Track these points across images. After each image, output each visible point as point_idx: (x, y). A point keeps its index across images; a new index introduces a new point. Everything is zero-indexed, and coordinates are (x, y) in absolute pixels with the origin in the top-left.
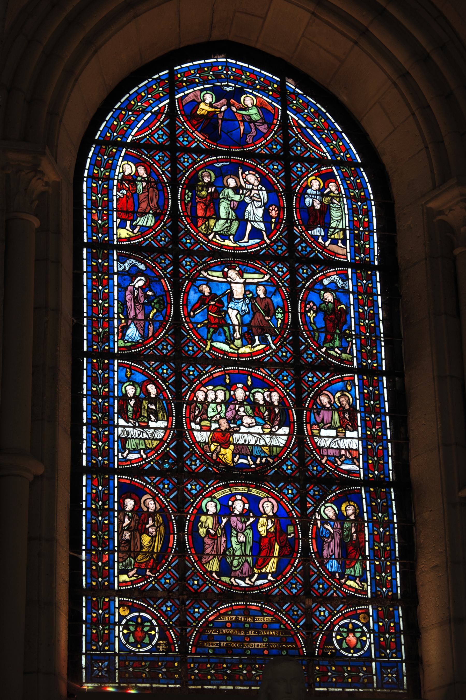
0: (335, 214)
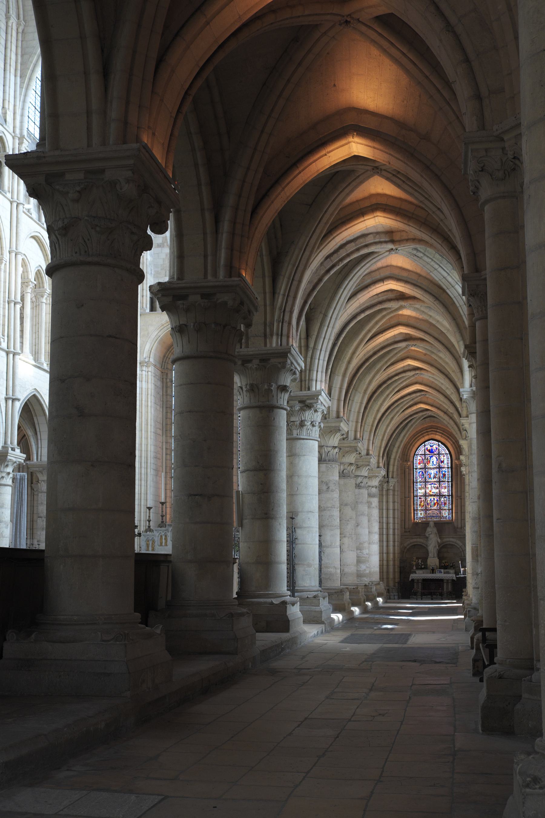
0: (445, 461)
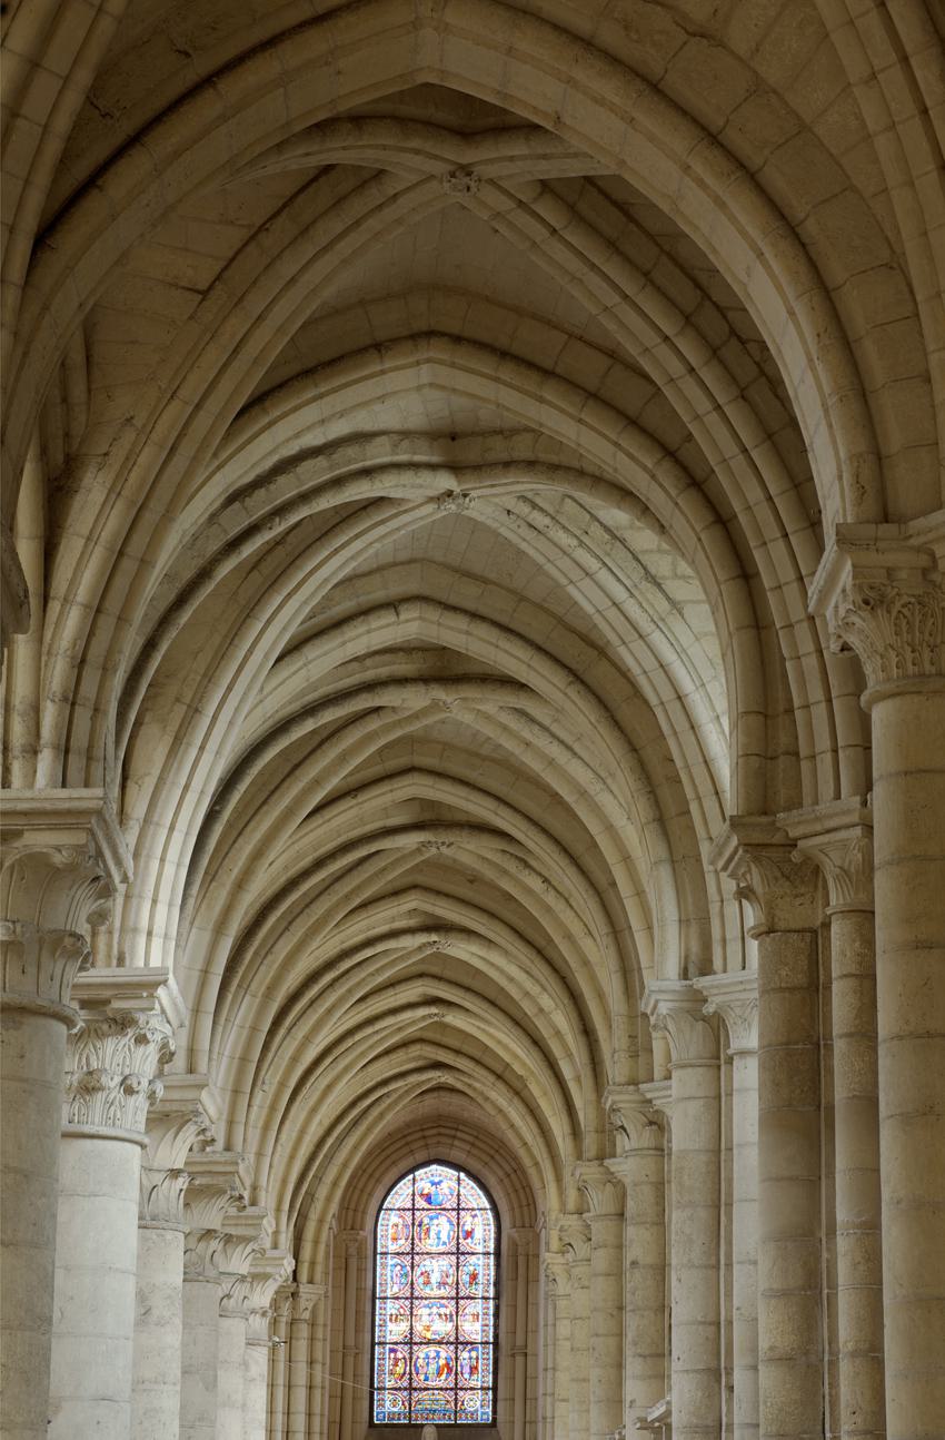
0: (476, 1232)
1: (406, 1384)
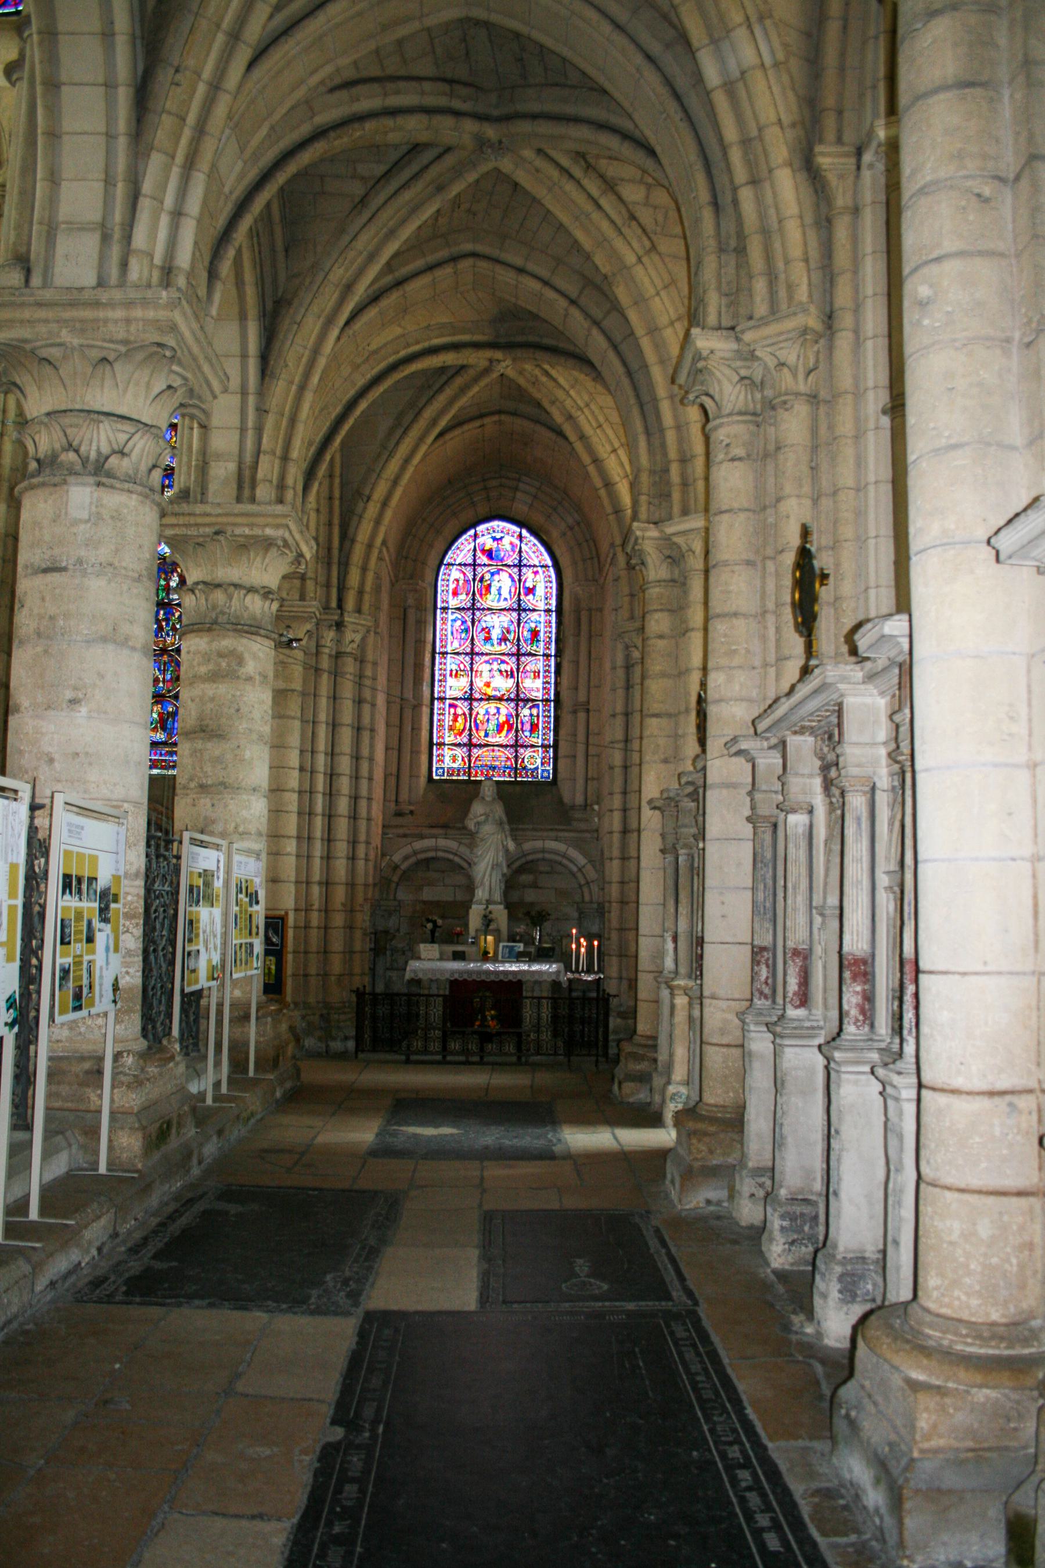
1: (465, 740)
